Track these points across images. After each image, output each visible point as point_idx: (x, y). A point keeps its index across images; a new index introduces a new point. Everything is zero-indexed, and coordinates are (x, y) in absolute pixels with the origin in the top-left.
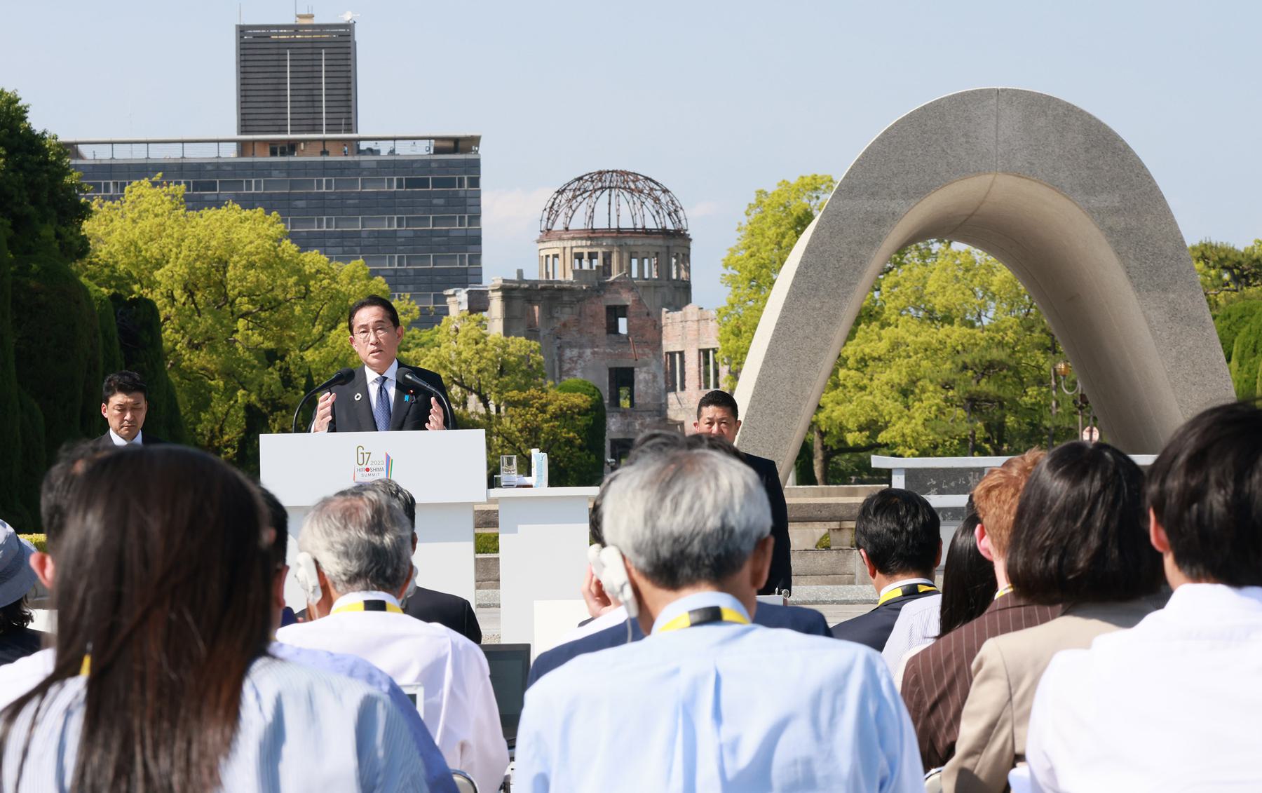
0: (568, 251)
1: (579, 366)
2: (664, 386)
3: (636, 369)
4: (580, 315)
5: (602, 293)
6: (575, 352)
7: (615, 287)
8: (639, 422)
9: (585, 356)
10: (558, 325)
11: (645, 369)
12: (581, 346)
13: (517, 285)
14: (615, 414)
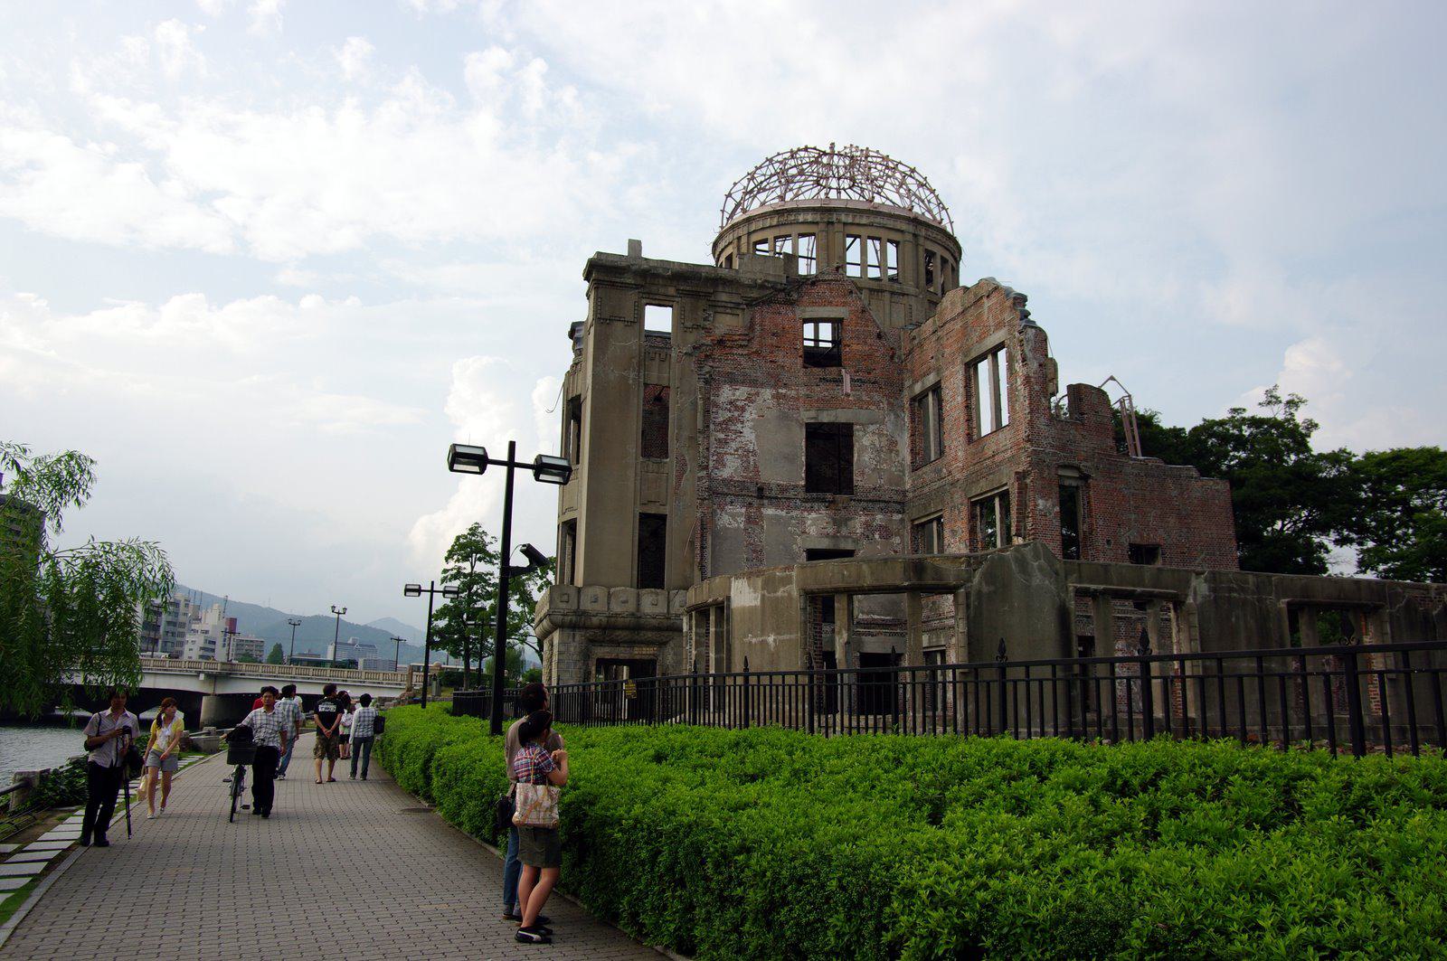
0: (744, 240)
1: (747, 415)
2: (908, 459)
3: (856, 427)
4: (751, 327)
5: (795, 296)
6: (742, 392)
7: (816, 289)
8: (863, 519)
9: (759, 400)
10: (708, 341)
11: (872, 428)
12: (753, 383)
13: (624, 264)
14: (816, 506)
